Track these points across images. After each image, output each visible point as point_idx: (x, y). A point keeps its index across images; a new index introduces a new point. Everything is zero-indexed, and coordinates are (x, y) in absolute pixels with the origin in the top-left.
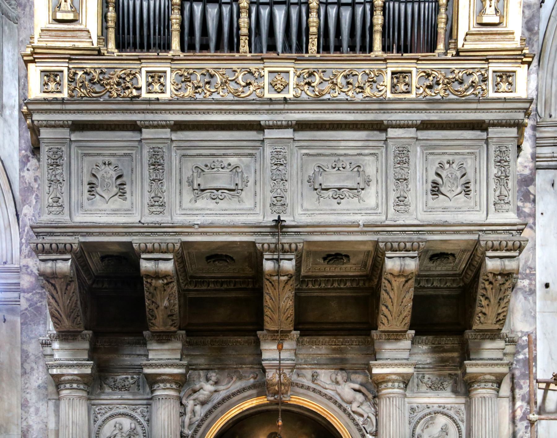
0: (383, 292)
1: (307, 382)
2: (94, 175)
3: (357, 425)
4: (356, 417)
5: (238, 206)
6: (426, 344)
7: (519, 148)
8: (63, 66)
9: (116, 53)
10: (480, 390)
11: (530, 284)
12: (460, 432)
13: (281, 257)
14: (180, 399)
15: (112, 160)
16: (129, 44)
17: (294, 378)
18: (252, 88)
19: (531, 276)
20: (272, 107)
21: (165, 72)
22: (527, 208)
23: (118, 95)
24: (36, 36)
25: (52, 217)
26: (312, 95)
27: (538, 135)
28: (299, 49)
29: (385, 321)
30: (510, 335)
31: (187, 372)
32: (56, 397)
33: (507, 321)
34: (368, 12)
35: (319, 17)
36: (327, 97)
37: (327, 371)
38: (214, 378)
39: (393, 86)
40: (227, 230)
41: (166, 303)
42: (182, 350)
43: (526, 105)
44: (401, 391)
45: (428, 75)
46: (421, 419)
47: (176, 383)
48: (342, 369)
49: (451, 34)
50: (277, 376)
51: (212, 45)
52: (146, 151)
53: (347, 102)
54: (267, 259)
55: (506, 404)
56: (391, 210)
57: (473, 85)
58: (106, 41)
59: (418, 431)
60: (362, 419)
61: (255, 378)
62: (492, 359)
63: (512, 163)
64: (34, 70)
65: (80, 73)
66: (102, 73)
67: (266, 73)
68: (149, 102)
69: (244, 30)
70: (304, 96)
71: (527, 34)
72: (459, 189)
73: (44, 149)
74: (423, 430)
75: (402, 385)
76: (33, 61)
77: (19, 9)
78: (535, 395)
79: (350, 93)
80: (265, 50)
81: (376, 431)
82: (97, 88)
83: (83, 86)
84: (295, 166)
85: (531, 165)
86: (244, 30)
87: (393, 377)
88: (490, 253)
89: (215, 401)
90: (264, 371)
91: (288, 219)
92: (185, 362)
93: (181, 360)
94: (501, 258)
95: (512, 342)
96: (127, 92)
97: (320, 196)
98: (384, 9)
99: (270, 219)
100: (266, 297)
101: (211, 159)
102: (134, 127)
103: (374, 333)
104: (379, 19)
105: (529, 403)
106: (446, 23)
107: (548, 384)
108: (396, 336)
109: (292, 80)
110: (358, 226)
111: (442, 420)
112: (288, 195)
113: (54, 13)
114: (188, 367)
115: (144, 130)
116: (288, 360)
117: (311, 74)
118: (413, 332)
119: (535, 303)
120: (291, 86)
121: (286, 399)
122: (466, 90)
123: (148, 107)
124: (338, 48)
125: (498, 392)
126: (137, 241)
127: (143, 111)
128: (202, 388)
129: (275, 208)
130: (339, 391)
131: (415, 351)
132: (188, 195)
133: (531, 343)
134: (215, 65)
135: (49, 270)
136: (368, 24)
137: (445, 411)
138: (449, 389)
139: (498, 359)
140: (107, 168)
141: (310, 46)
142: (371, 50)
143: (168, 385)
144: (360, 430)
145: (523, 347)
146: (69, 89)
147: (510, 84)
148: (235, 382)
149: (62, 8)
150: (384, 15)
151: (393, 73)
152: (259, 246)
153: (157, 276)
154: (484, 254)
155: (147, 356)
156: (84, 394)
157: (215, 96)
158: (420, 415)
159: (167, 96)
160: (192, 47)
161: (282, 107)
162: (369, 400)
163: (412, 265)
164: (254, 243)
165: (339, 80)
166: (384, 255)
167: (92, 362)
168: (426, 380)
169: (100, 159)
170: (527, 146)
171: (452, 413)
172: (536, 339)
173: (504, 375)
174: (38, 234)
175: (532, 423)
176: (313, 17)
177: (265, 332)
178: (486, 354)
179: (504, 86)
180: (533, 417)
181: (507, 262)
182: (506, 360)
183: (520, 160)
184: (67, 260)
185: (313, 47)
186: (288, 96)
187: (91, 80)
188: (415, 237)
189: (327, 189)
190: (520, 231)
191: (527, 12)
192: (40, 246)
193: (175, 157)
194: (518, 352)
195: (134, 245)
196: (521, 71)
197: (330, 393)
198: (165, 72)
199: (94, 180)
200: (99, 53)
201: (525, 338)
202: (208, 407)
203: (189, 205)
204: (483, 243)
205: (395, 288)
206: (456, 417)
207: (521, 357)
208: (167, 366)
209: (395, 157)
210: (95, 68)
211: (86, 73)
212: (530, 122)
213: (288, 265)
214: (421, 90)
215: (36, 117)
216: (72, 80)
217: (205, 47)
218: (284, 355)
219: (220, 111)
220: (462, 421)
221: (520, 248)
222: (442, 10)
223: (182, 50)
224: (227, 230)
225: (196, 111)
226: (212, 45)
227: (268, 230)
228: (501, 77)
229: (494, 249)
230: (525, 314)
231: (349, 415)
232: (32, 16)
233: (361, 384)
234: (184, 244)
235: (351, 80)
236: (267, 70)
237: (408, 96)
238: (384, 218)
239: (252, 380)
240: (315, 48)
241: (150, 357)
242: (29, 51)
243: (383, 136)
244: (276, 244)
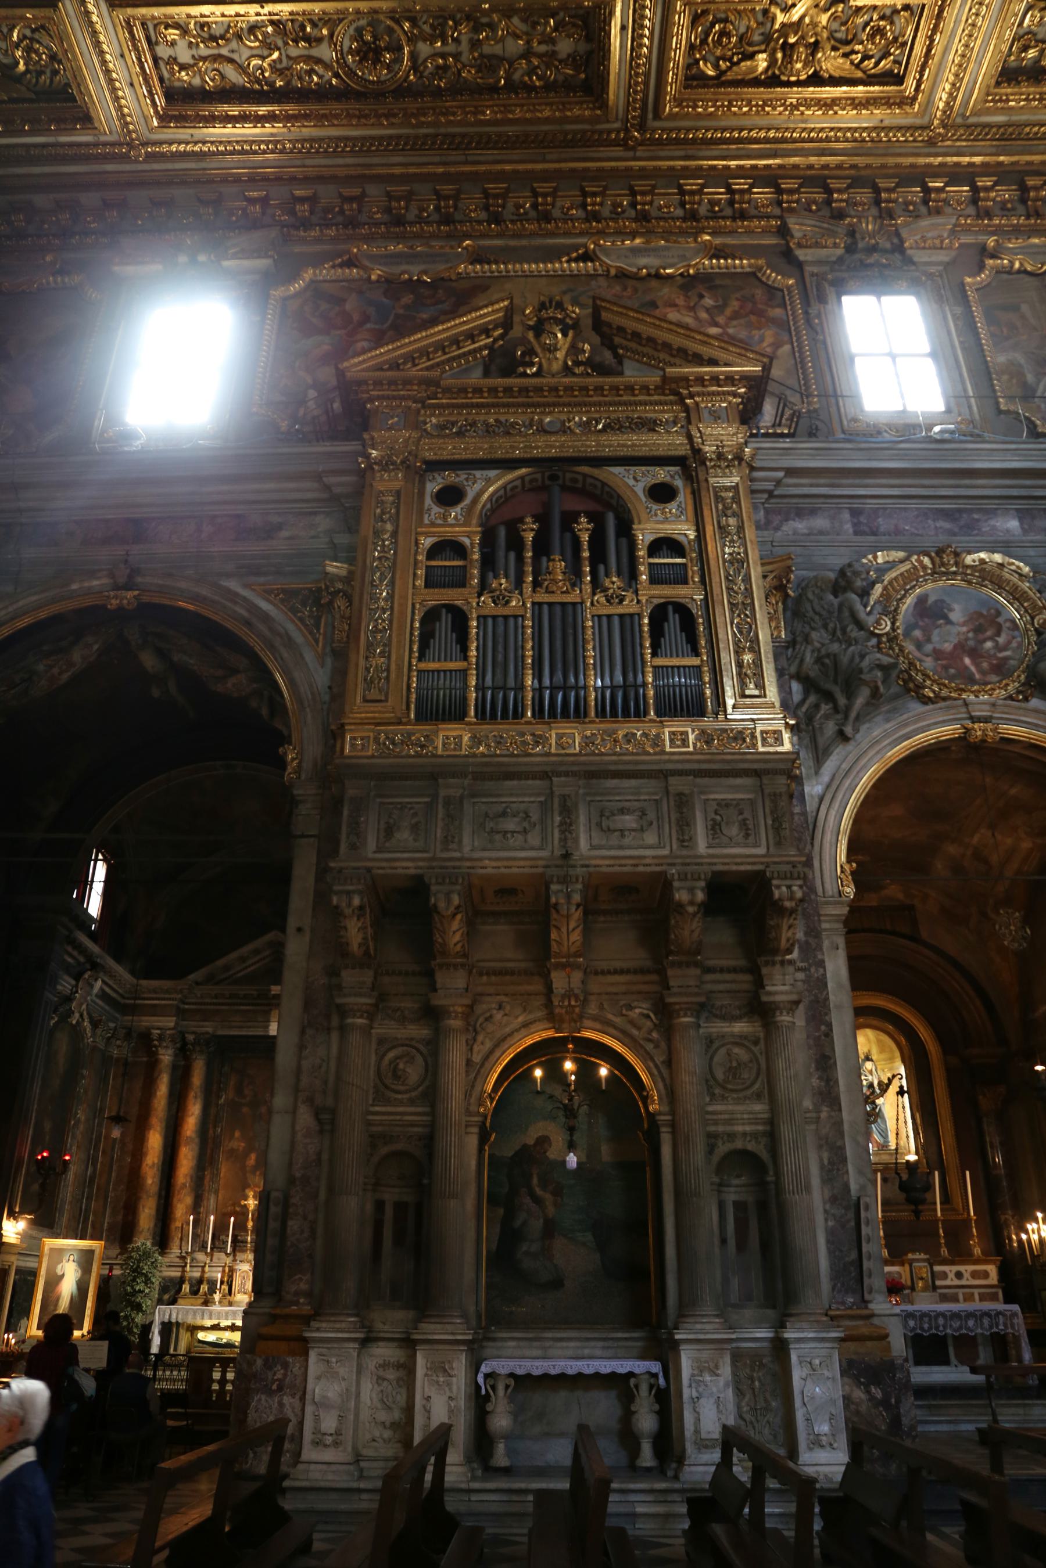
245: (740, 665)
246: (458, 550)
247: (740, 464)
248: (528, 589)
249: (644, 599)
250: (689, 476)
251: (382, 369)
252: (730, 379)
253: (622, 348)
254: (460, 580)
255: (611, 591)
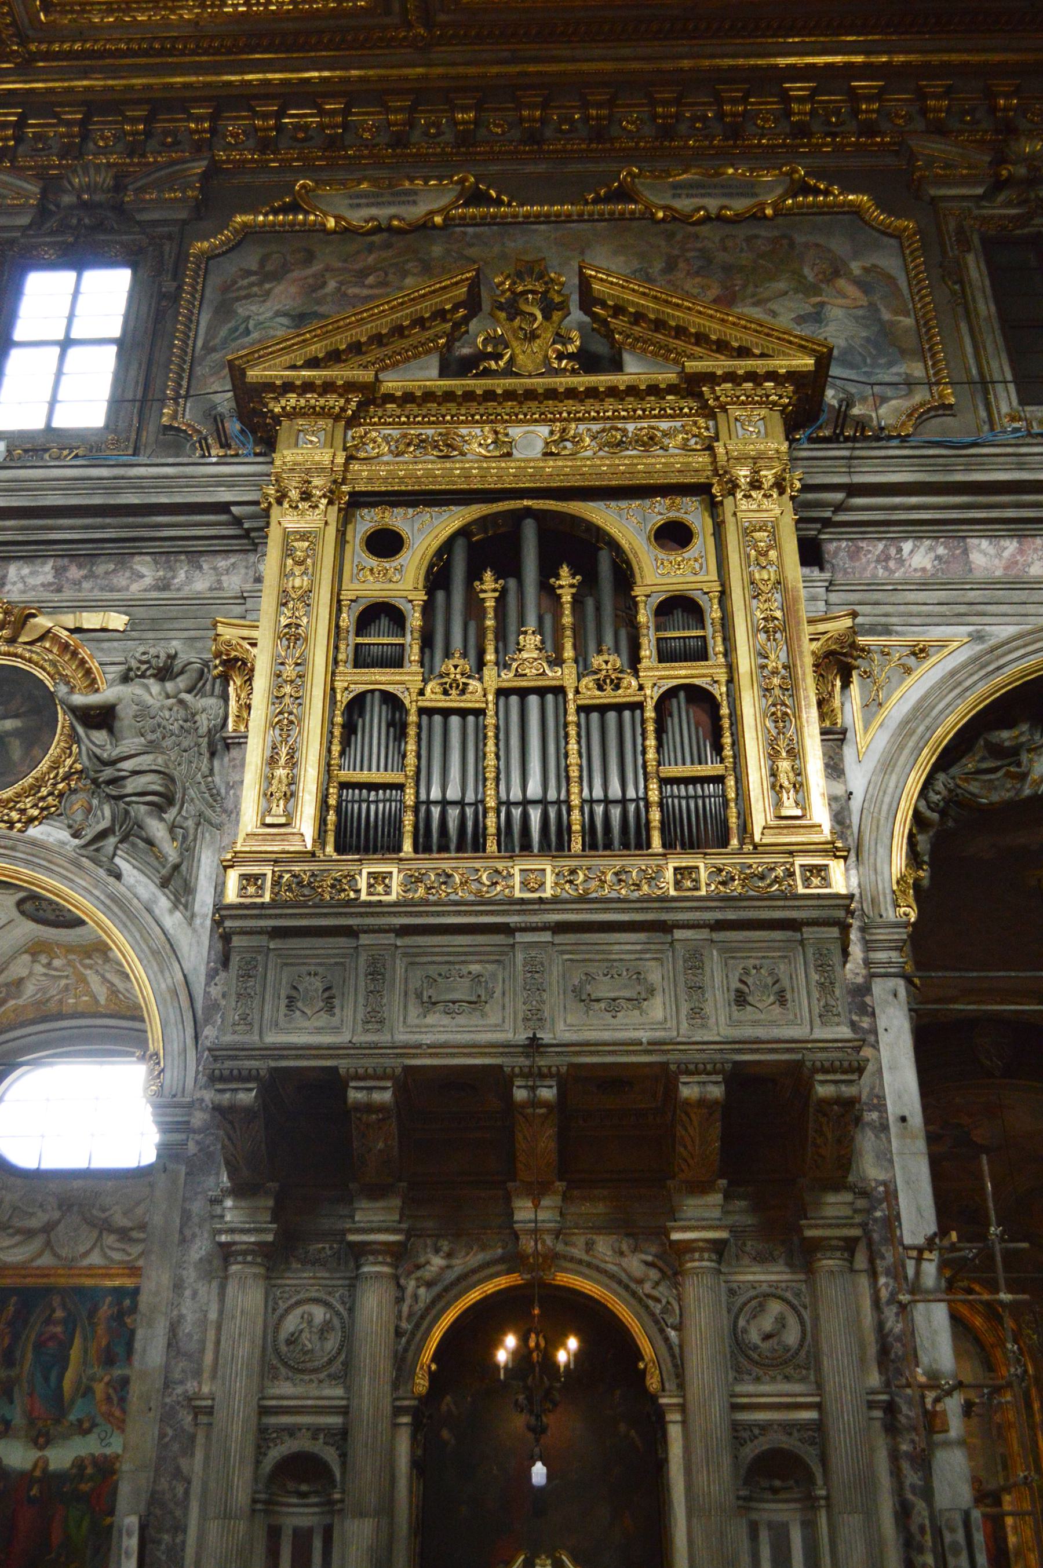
0: (679, 1128)
1: (578, 1252)
2: (295, 988)
3: (652, 1314)
4: (651, 1303)
5: (481, 1022)
6: (745, 1199)
7: (845, 953)
8: (268, 870)
9: (335, 856)
10: (825, 1262)
11: (881, 1117)
12: (802, 1323)
13: (538, 1083)
14: (396, 1278)
15: (320, 970)
16: (351, 848)
17: (560, 1247)
18: (499, 888)
19: (881, 1107)
20: (524, 907)
21: (391, 873)
22: (865, 1023)
23: (332, 898)
24: (240, 841)
25: (236, 1038)
26: (575, 894)
27: (868, 937)
28: (560, 847)
29: (684, 1167)
30: (860, 1185)
31: (408, 1239)
32: (221, 1274)
33: (854, 1166)
34: (643, 810)
35: (583, 814)
36: (594, 895)
37: (606, 1238)
38: (446, 1249)
39: (677, 884)
40: (465, 1051)
41: (381, 1145)
42: (402, 1209)
43: (847, 902)
44: (713, 1264)
45: (720, 870)
46: (745, 1304)
47: (392, 1255)
48: (627, 1235)
49: (745, 828)
50: (532, 1243)
51: (453, 846)
52: (362, 960)
53: (619, 900)
54: (519, 1087)
55: (864, 1281)
56: (684, 1025)
57: (776, 880)
58: (323, 845)
59: (742, 1323)
60: (659, 1306)
61: (503, 1248)
62: (838, 1218)
63: (838, 968)
64: (233, 877)
65: (287, 876)
66: (313, 875)
67: (516, 872)
68: (369, 904)
69: (492, 830)
70: (565, 895)
71: (838, 828)
72: (772, 999)
73: (235, 960)
74: (748, 1322)
75: (714, 1257)
76: (232, 867)
77: (224, 816)
78: (904, 1267)
79: (623, 892)
80: (517, 850)
81: (681, 1323)
82: (306, 891)
83: (290, 890)
84: (555, 973)
85: (864, 972)
86: (492, 830)
87: (701, 1244)
88: (820, 1077)
89: (447, 1282)
90: (517, 1238)
91: (546, 1036)
92: (404, 1226)
93: (400, 1222)
94: (836, 1082)
95: (864, 1194)
96: (343, 895)
97: (588, 1009)
98: (661, 805)
99: (522, 1036)
100: (519, 1137)
101: (446, 967)
102: (350, 932)
103: (670, 1183)
104: (655, 815)
105: (895, 1278)
106: (738, 818)
107: (920, 1250)
108: (702, 1188)
109: (550, 879)
110: (641, 1044)
111: (775, 1307)
112: (546, 1008)
113: (263, 817)
114: (409, 1233)
115: (361, 936)
116: (550, 1221)
117: (573, 872)
118: (723, 1182)
119: (890, 1142)
120: (549, 884)
121: (547, 1278)
122: (770, 885)
123: (368, 910)
124: (608, 846)
125: (851, 1262)
126: (343, 1064)
127: (361, 915)
128: (428, 1263)
129: (529, 1024)
130: (624, 1265)
131: (731, 1208)
132: (413, 1011)
133: (891, 1195)
134: (454, 864)
135: (225, 1103)
136: (643, 821)
137: (779, 1292)
138: (781, 1261)
139: (847, 1218)
140: (312, 979)
141: (573, 844)
142: (649, 846)
143: (380, 1259)
144: (656, 1322)
145: (880, 1202)
146: (272, 893)
147: (823, 879)
148: (475, 1255)
149: (273, 812)
150: (662, 811)
151: (676, 869)
152: (507, 1070)
153: (369, 1108)
154: (811, 1077)
155: (352, 1217)
156: (261, 1270)
157: (453, 897)
158: (741, 1300)
159: (393, 897)
160: (428, 849)
161: (536, 907)
162: (669, 1278)
163: (716, 1092)
164: (500, 1067)
165: (609, 877)
166: (677, 1080)
167: (275, 1226)
168: (748, 1248)
169: (304, 969)
170: (856, 950)
171: (788, 1295)
172: (896, 1190)
173: (856, 1240)
174: (216, 1059)
175: (903, 1307)
176: (576, 815)
177: (518, 1184)
178: (829, 1212)
179: (816, 881)
180: (904, 1298)
181: (843, 1088)
182: (858, 1219)
183: (848, 966)
184: (250, 1090)
185: (577, 845)
186: (543, 895)
187: (298, 884)
188: (718, 1057)
189: (598, 1000)
190: (858, 1049)
191: (834, 805)
192: (217, 1072)
193: (400, 966)
194: (874, 1208)
195: (341, 1071)
196: (837, 869)
197: (610, 1267)
198: (391, 873)
199: (294, 993)
200: (313, 854)
201: (881, 1189)
202: (436, 1289)
203: (417, 1021)
204: (809, 1064)
205: (696, 1123)
206: (796, 1302)
207: (878, 1214)
208: (380, 1230)
209: (685, 961)
210: (305, 872)
211: (294, 876)
212: (856, 923)
213: (547, 1094)
214: (713, 887)
215: (228, 923)
216: (276, 883)
217: (444, 848)
218: (542, 1216)
219: (459, 913)
220: (805, 1307)
221: (860, 1070)
222: (732, 805)
223: (416, 850)
224: (465, 1051)
225: (427, 914)
226: (453, 846)
227: (520, 1050)
228: (811, 871)
229: (825, 1071)
230: (878, 1157)
231: (640, 1300)
232: (238, 822)
233: (655, 1256)
234: (407, 1069)
235: (624, 877)
236: (517, 868)
237: (696, 893)
238: (675, 1034)
239: (500, 1251)
240: (580, 846)
241: (357, 1218)
242: (229, 856)
243: (669, 938)
244: (531, 1067)
245: (774, 774)
246: (396, 617)
247: (781, 493)
248: (490, 672)
249: (648, 685)
250: (714, 507)
251: (293, 367)
252: (772, 376)
253: (620, 334)
254: (395, 660)
255: (604, 673)
